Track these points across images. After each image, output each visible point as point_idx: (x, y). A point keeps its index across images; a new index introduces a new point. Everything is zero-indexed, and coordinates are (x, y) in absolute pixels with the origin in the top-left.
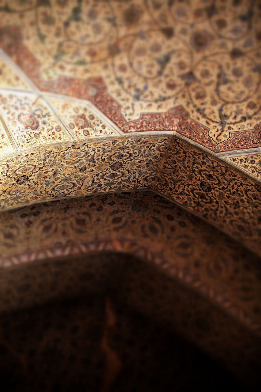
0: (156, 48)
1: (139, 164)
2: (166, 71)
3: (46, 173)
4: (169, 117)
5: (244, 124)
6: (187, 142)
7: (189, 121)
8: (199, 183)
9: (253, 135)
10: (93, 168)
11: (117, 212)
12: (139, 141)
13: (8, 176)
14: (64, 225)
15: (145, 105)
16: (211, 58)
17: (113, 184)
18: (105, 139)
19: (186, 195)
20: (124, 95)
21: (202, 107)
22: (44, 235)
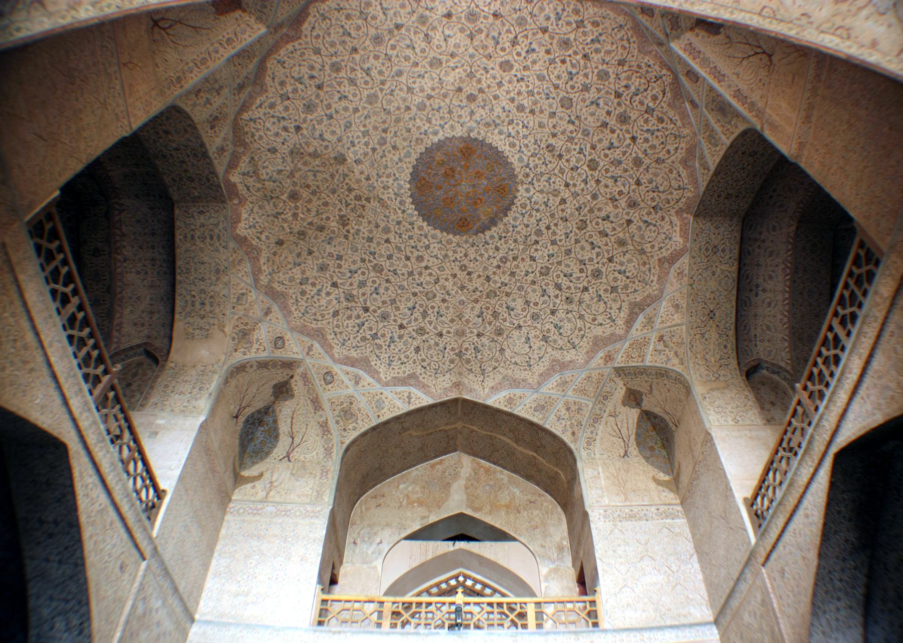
0: (639, 228)
2: (654, 222)
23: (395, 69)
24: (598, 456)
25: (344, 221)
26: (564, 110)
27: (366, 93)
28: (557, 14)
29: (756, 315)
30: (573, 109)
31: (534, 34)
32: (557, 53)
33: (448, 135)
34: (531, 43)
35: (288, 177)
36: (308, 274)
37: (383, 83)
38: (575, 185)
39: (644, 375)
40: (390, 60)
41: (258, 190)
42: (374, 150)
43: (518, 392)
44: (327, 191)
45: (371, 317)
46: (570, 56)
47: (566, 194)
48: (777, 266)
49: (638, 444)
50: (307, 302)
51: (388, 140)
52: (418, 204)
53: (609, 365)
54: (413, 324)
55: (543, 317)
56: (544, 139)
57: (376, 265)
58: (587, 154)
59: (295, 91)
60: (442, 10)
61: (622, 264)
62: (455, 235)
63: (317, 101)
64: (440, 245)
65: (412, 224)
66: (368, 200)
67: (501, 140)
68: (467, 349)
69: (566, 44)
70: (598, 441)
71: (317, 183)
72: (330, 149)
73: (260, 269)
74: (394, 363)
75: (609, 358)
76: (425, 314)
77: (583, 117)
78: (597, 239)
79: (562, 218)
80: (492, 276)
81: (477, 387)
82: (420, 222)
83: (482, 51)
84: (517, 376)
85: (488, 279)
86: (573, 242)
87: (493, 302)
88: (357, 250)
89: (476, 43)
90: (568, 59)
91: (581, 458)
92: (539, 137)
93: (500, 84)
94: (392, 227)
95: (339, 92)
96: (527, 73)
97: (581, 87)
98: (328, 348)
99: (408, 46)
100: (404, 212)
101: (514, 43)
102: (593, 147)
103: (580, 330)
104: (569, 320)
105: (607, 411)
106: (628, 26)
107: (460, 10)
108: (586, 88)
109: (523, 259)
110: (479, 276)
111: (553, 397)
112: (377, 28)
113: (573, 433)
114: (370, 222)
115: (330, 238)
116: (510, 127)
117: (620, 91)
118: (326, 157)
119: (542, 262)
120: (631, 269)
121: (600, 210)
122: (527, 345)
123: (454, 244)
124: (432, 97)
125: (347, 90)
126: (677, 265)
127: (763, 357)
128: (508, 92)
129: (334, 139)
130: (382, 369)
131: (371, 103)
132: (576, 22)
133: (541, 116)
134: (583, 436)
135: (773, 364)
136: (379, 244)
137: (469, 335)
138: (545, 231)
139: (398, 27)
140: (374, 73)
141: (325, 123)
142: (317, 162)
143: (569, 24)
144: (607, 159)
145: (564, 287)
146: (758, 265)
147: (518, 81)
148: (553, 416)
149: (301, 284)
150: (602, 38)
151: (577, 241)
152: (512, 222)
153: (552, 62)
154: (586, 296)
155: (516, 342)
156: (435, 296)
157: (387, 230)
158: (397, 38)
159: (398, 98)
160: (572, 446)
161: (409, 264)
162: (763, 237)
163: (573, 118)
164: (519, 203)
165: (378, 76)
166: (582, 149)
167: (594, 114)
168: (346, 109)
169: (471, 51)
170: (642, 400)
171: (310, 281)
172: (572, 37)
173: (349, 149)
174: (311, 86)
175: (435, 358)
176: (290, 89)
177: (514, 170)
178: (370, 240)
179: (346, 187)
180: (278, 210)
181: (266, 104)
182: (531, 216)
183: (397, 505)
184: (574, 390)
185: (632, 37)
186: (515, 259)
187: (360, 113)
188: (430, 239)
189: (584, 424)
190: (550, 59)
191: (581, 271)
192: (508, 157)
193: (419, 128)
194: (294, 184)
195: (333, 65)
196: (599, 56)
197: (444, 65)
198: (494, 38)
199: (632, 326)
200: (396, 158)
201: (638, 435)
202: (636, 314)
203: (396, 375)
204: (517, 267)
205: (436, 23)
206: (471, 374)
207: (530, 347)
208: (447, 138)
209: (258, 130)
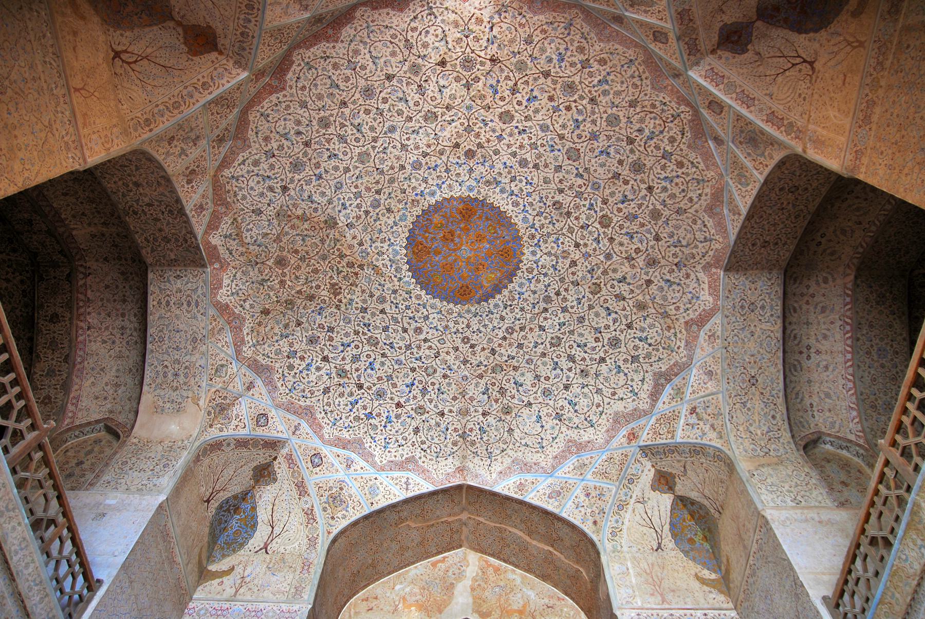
0: (661, 289)
2: (677, 281)
4: (711, 276)
9: (716, 219)
11: (817, 281)
13: (746, 393)
14: (824, 323)
15: (702, 293)
18: (723, 325)
20: (696, 307)
22: (831, 339)
23: (387, 125)
24: (625, 549)
25: (335, 290)
26: (570, 162)
27: (357, 150)
28: (560, 54)
29: (809, 381)
31: (535, 79)
32: (562, 99)
33: (446, 196)
34: (532, 90)
35: (274, 241)
36: (296, 346)
37: (375, 140)
38: (586, 245)
39: (676, 454)
40: (381, 114)
41: (242, 254)
42: (367, 213)
43: (529, 477)
44: (316, 257)
45: (366, 395)
46: (575, 101)
47: (576, 255)
48: (832, 323)
49: (674, 536)
50: (294, 377)
51: (382, 202)
52: (416, 271)
53: (633, 443)
54: (411, 402)
55: (556, 393)
56: (550, 196)
57: (371, 337)
58: (598, 209)
59: (281, 148)
60: (435, 58)
61: (642, 330)
62: (456, 304)
63: (305, 160)
64: (439, 316)
65: (408, 293)
66: (361, 267)
67: (503, 199)
68: (471, 430)
69: (570, 88)
70: (625, 531)
71: (305, 248)
72: (320, 212)
73: (243, 338)
74: (391, 445)
75: (632, 436)
76: (424, 391)
77: (592, 169)
78: (612, 304)
79: (572, 283)
80: (498, 349)
81: (483, 472)
82: (418, 291)
83: (479, 102)
84: (528, 460)
85: (493, 352)
86: (586, 308)
87: (499, 377)
88: (349, 322)
90: (573, 105)
91: (605, 550)
92: (544, 193)
93: (500, 138)
94: (388, 297)
95: (328, 150)
96: (529, 124)
97: (588, 136)
98: (317, 428)
99: (401, 99)
100: (400, 279)
101: (514, 91)
102: (605, 202)
103: (598, 406)
104: (585, 396)
105: (634, 497)
108: (594, 137)
109: (531, 329)
110: (483, 349)
111: (570, 481)
112: (366, 80)
113: (595, 523)
114: (363, 291)
115: (321, 308)
116: (513, 185)
117: (633, 136)
118: (316, 220)
119: (552, 332)
120: (653, 335)
121: (615, 271)
122: (539, 425)
123: (455, 315)
124: (428, 154)
125: (336, 147)
126: (707, 327)
127: (824, 430)
128: (509, 146)
129: (324, 200)
130: (377, 452)
131: (362, 162)
133: (546, 170)
134: (608, 525)
135: (839, 438)
136: (373, 314)
137: (473, 414)
138: (554, 297)
139: (389, 77)
140: (365, 129)
141: (314, 183)
142: (306, 226)
143: (573, 65)
144: (621, 214)
145: (578, 358)
146: (808, 323)
147: (519, 133)
148: (570, 503)
149: (289, 357)
150: (609, 78)
151: (591, 307)
152: (517, 288)
153: (556, 109)
154: (604, 368)
155: (526, 421)
156: (435, 371)
157: (382, 300)
158: (389, 90)
159: (392, 156)
160: (595, 538)
161: (407, 337)
162: (811, 291)
163: (581, 170)
164: (525, 267)
165: (369, 133)
166: (592, 205)
167: (605, 165)
168: (336, 168)
169: (468, 102)
170: (675, 484)
171: (298, 355)
172: (577, 79)
173: (340, 211)
174: (297, 142)
175: (436, 440)
176: (275, 145)
177: (518, 231)
178: (364, 310)
179: (337, 253)
180: (264, 277)
181: (250, 161)
182: (538, 281)
183: (391, 609)
184: (594, 473)
185: (644, 72)
186: (522, 329)
187: (352, 173)
188: (429, 309)
189: (606, 511)
190: (553, 107)
191: (597, 340)
192: (511, 217)
193: (414, 188)
194: (282, 249)
195: (321, 120)
196: (607, 98)
197: (439, 119)
198: (492, 86)
199: (658, 399)
200: (390, 222)
201: (672, 525)
202: (662, 385)
203: (393, 458)
204: (525, 338)
205: (429, 73)
206: (476, 458)
207: (542, 427)
208: (445, 199)
209: (241, 189)
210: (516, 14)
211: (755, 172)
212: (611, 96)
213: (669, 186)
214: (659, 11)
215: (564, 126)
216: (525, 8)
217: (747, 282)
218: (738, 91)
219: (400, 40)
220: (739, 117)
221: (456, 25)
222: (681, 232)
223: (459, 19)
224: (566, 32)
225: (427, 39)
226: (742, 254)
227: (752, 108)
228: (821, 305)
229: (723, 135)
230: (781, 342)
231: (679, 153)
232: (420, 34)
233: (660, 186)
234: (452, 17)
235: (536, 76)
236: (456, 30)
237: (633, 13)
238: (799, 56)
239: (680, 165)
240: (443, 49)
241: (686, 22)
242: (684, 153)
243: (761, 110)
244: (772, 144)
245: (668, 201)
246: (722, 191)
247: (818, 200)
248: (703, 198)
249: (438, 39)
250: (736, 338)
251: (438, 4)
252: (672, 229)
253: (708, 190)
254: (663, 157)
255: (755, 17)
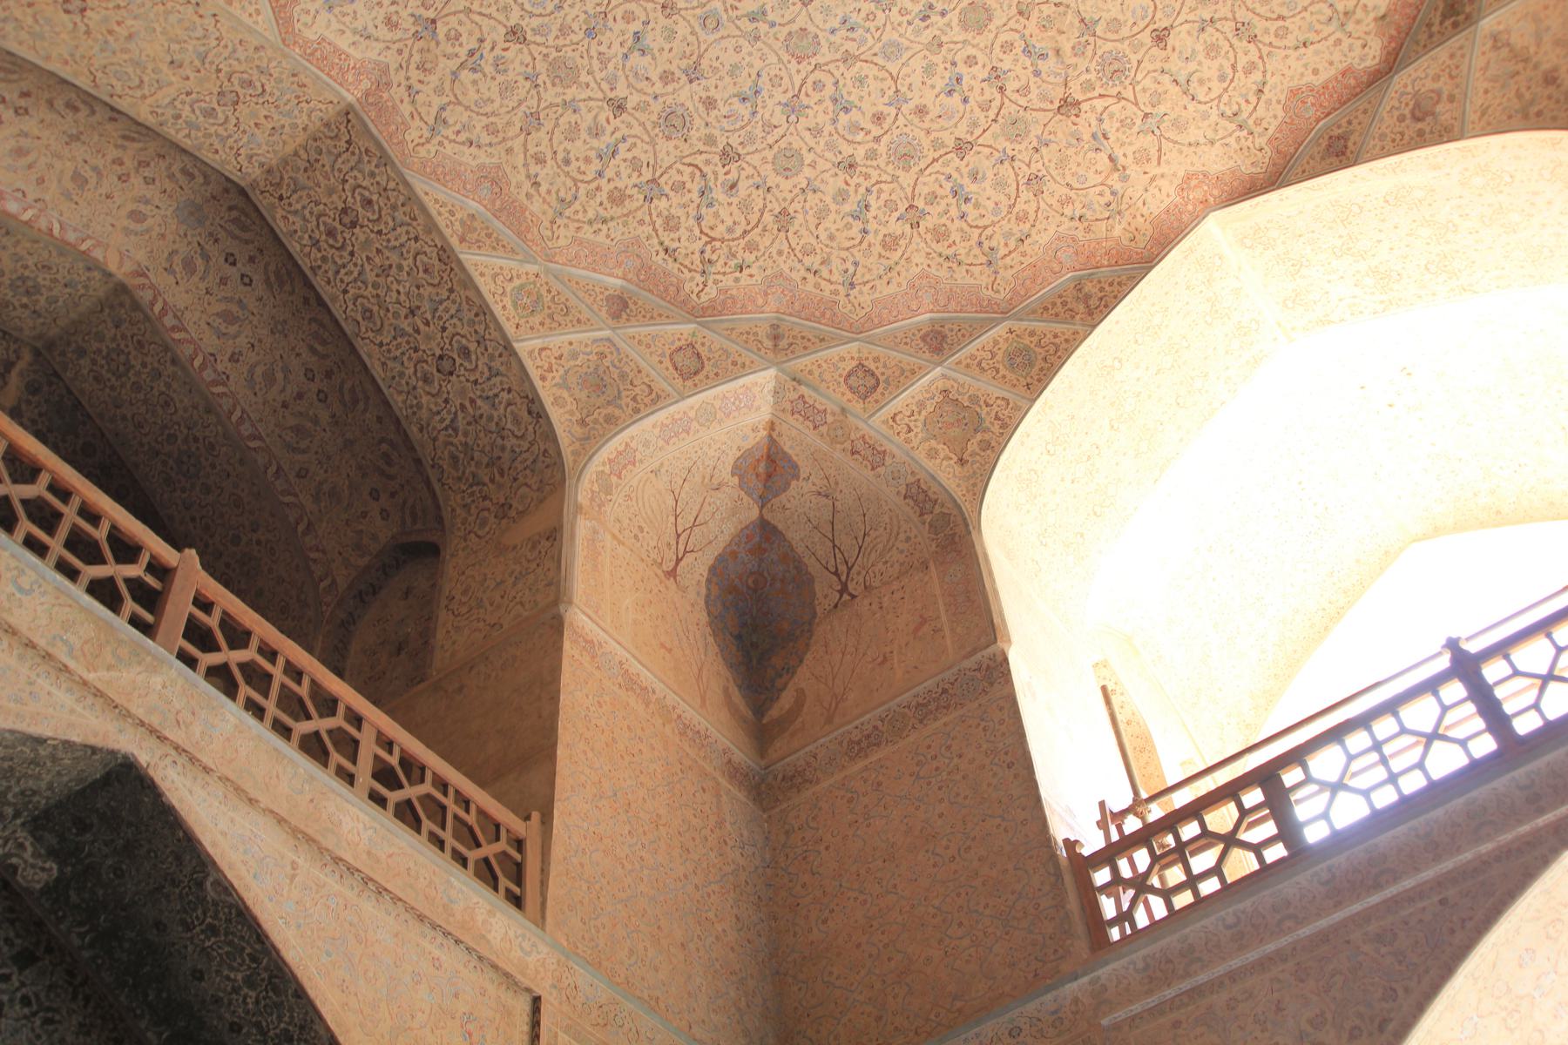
1: (263, 121)
3: (119, 23)
5: (465, 148)
6: (365, 125)
7: (385, 96)
8: (341, 206)
10: (192, 75)
11: (147, 202)
12: (294, 75)
14: (50, 166)
16: (477, 18)
17: (198, 129)
18: (250, 30)
19: (304, 219)
21: (417, 86)
26: (795, 27)
28: (967, 200)
30: (777, 45)
34: (965, 101)
46: (877, 139)
48: (41, 181)
60: (1181, 38)
69: (905, 158)
77: (746, 48)
89: (1071, 17)
96: (926, 36)
97: (805, 101)
101: (996, 75)
106: (841, 298)
107: (1146, 65)
108: (793, 108)
117: (734, 167)
132: (924, 214)
143: (933, 198)
144: (619, 13)
146: (75, 138)
147: (931, 7)
153: (898, 99)
162: (136, 181)
163: (763, 27)
167: (731, 74)
172: (906, 179)
185: (817, 286)
198: (1043, 56)
210: (1089, 214)
211: (537, 343)
212: (828, 199)
213: (595, 143)
214: (910, 430)
215: (861, 81)
216: (1080, 234)
217: (286, 121)
218: (695, 424)
219: (1266, 31)
220: (656, 400)
221: (1178, 125)
222: (490, 89)
223: (1178, 138)
224: (986, 245)
225: (1216, 64)
226: (367, 169)
227: (657, 431)
228: (93, 181)
229: (631, 330)
230: (107, 99)
231: (639, 215)
232: (1234, 67)
233: (609, 129)
234: (1194, 134)
235: (978, 132)
236: (1173, 116)
237: (932, 382)
238: (685, 552)
239: (618, 198)
240: (1175, 65)
241: (859, 445)
242: (633, 223)
243: (646, 444)
244: (582, 423)
245: (569, 117)
246: (519, 234)
247: (377, 372)
248: (527, 186)
249: (1194, 79)
250: (199, 33)
251: (1231, 140)
252: (511, 76)
253: (536, 206)
254: (654, 181)
255: (768, 516)
